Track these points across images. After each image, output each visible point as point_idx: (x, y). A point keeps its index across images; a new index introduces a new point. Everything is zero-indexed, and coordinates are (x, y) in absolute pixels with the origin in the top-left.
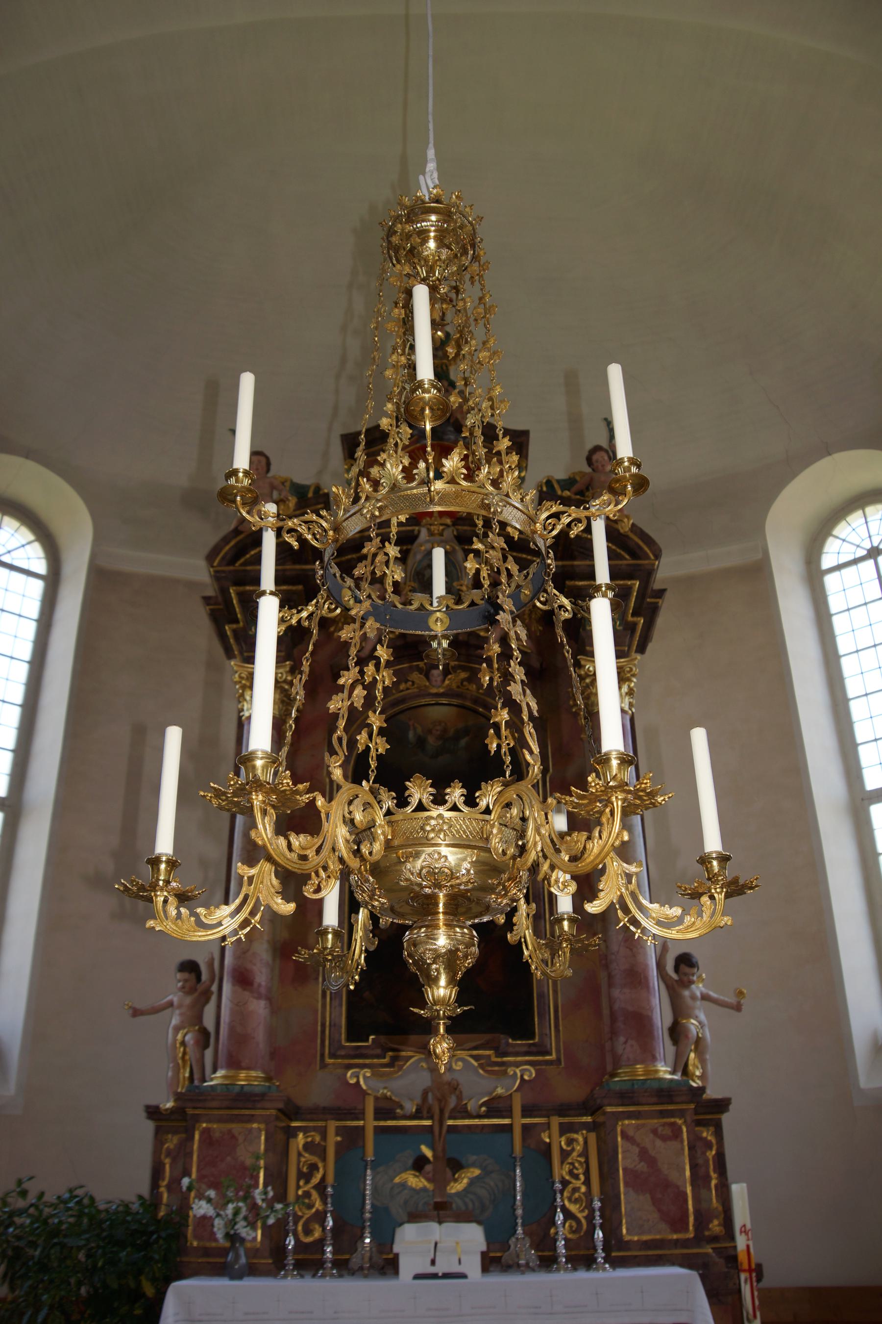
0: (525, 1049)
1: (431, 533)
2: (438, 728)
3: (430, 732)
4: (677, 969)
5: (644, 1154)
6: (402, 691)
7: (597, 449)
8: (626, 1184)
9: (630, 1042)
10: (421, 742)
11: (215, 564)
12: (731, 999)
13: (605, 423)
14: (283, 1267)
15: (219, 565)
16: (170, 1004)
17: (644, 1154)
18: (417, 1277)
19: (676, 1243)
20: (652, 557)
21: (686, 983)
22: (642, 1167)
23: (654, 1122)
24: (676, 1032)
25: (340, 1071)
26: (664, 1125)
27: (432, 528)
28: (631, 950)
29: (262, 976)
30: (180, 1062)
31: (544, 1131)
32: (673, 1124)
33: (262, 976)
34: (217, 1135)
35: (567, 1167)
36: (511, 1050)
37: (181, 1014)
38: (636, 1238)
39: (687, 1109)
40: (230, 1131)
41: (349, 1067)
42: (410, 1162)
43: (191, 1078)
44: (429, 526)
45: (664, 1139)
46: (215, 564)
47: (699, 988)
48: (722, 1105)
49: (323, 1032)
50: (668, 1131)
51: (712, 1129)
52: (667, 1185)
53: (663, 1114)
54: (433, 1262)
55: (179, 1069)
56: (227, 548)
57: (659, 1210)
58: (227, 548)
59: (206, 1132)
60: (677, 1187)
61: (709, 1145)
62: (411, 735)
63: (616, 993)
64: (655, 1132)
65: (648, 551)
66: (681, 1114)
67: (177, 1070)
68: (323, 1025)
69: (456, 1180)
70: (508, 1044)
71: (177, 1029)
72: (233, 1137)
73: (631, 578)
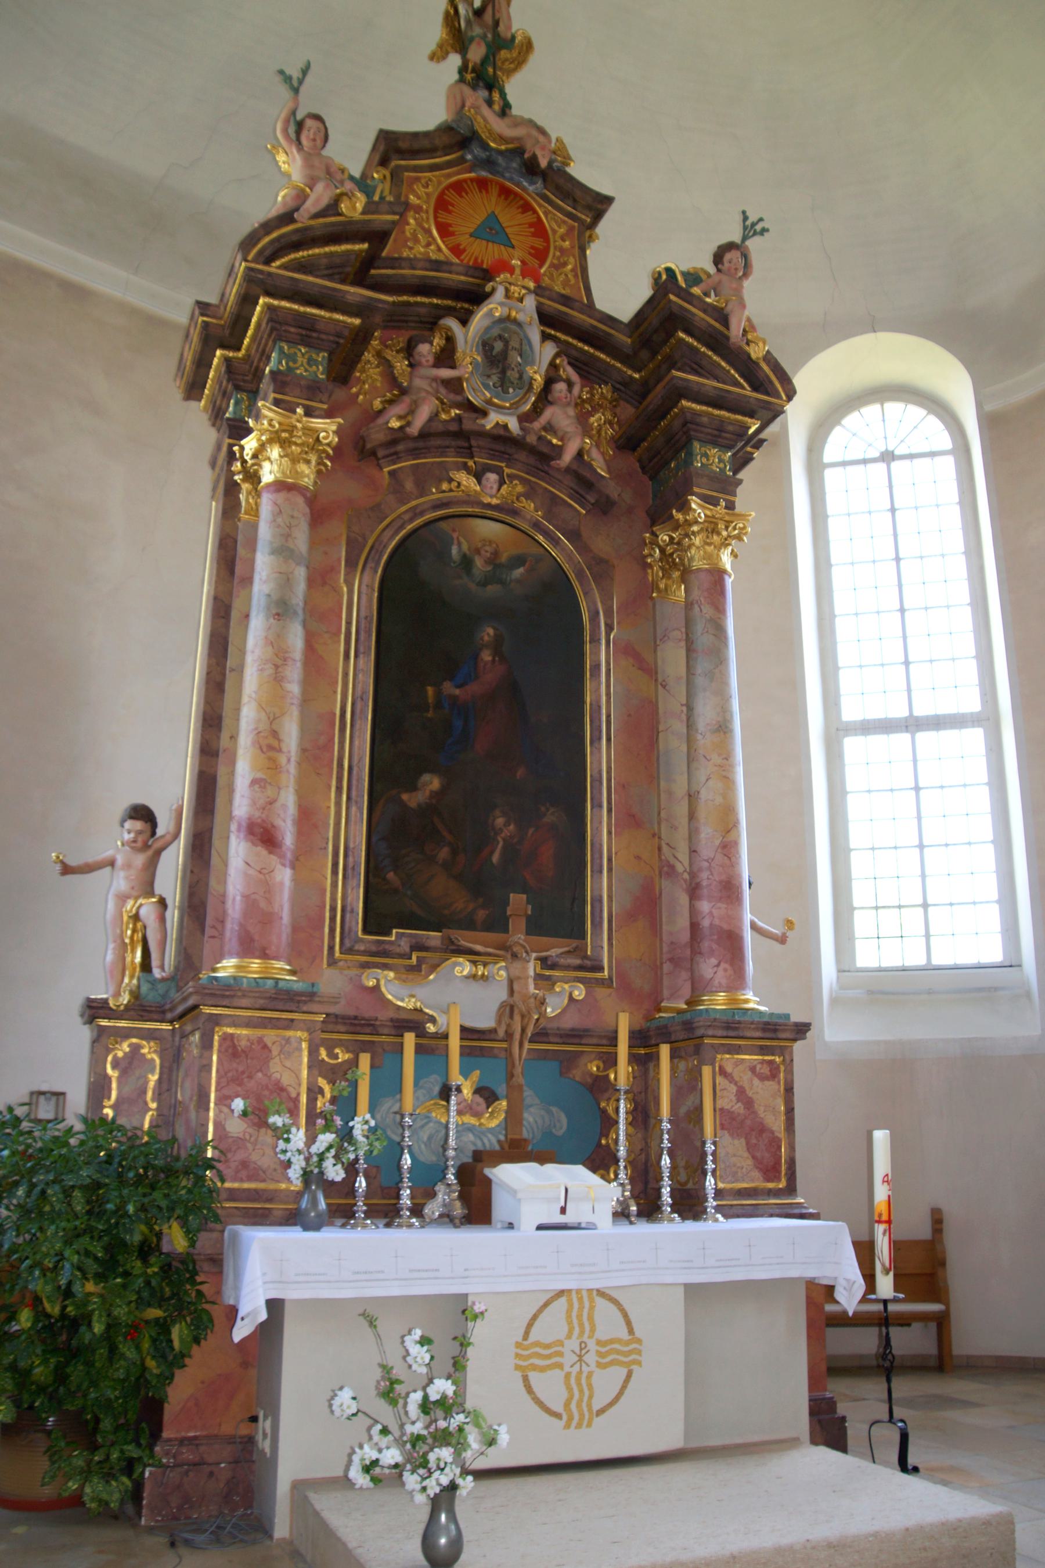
1: (508, 295)
2: (487, 548)
3: (478, 551)
5: (741, 1093)
6: (444, 492)
7: (730, 246)
9: (723, 965)
10: (467, 562)
11: (250, 258)
13: (742, 217)
14: (352, 1215)
17: (741, 1093)
18: (540, 1228)
20: (784, 397)
22: (739, 1108)
25: (354, 972)
26: (763, 1062)
27: (512, 288)
28: (730, 858)
30: (127, 941)
31: (591, 1062)
32: (771, 1062)
33: (288, 838)
34: (244, 1043)
37: (127, 878)
38: (729, 1186)
40: (260, 1040)
41: (365, 966)
42: (437, 1089)
44: (508, 285)
45: (762, 1078)
46: (250, 258)
49: (333, 919)
50: (766, 1070)
52: (762, 1129)
54: (563, 1211)
55: (125, 951)
56: (267, 240)
57: (754, 1157)
58: (267, 240)
59: (227, 1038)
60: (772, 1132)
62: (454, 550)
64: (753, 1069)
65: (780, 390)
68: (333, 909)
71: (123, 898)
72: (265, 1047)
73: (752, 415)
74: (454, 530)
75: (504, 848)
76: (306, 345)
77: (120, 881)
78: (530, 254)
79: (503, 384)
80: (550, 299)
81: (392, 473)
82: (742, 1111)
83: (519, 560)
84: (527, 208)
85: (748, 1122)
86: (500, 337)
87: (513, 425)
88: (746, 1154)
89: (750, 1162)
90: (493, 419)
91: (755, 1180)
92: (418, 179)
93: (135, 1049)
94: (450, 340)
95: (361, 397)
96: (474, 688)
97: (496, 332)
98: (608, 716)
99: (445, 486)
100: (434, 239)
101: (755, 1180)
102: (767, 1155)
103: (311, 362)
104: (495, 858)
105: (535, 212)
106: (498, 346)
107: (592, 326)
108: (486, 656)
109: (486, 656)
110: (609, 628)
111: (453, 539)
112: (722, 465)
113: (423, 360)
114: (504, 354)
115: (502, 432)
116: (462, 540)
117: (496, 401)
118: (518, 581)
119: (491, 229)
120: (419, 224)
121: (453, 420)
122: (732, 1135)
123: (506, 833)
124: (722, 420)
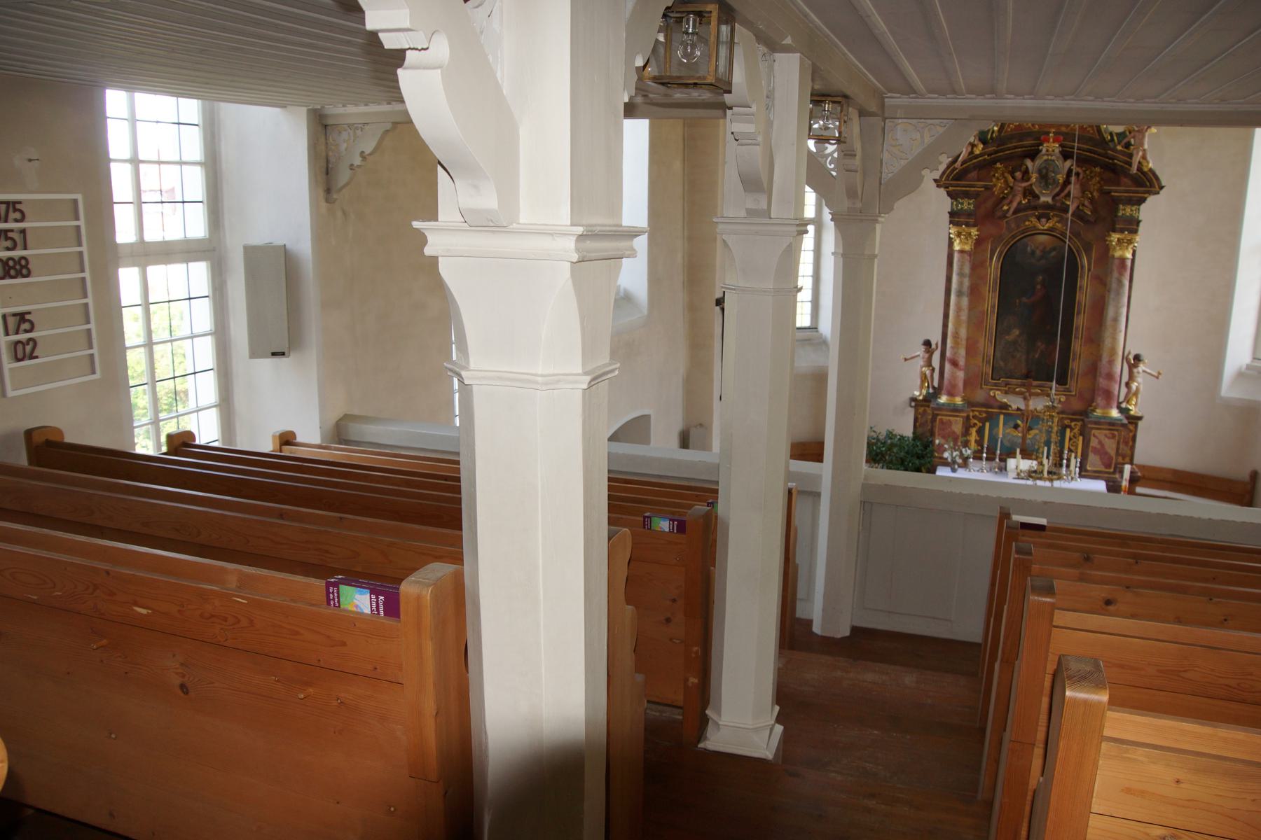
1: (1047, 151)
4: (1134, 360)
5: (1100, 443)
10: (1033, 253)
12: (1156, 374)
15: (945, 180)
16: (919, 356)
17: (1100, 443)
21: (1136, 366)
22: (1098, 447)
23: (1107, 432)
24: (1127, 385)
29: (962, 362)
33: (962, 362)
34: (944, 421)
35: (1072, 434)
41: (992, 389)
42: (1012, 425)
43: (928, 387)
45: (1109, 438)
47: (1141, 367)
48: (1140, 418)
50: (1111, 436)
51: (1134, 425)
52: (1106, 453)
61: (1131, 431)
62: (1029, 249)
63: (1101, 380)
64: (1106, 436)
67: (923, 382)
69: (1029, 434)
77: (922, 363)
81: (1007, 222)
83: (1054, 249)
86: (1045, 167)
89: (1100, 463)
90: (1043, 199)
91: (1102, 469)
93: (925, 410)
94: (1027, 168)
95: (996, 193)
97: (1043, 165)
99: (1027, 223)
101: (1102, 469)
103: (969, 204)
106: (1044, 171)
108: (1039, 287)
109: (1039, 287)
110: (1089, 270)
113: (1017, 179)
114: (1047, 174)
117: (1044, 192)
121: (1026, 203)
124: (1131, 197)
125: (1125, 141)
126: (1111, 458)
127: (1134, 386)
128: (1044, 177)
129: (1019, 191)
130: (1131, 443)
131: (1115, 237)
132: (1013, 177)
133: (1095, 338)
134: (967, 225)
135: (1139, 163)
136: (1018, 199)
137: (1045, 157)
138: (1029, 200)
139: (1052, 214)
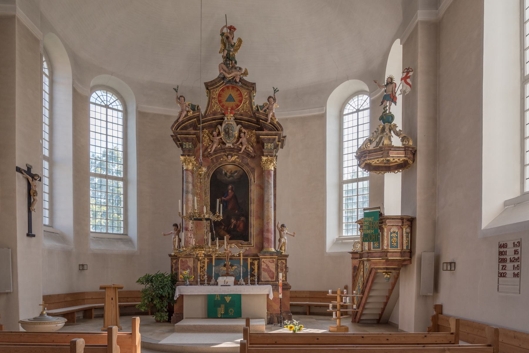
0: (247, 243)
5: (267, 265)
8: (263, 271)
10: (226, 174)
17: (267, 265)
18: (221, 286)
19: (272, 281)
22: (266, 268)
32: (273, 260)
36: (244, 244)
39: (276, 257)
45: (271, 263)
50: (272, 261)
52: (271, 271)
53: (271, 258)
62: (223, 172)
64: (269, 261)
66: (275, 258)
70: (243, 242)
73: (276, 135)
74: (223, 168)
75: (234, 225)
76: (188, 142)
78: (239, 102)
79: (229, 137)
80: (238, 116)
81: (211, 159)
82: (267, 268)
83: (236, 172)
84: (238, 90)
85: (268, 270)
87: (232, 146)
88: (267, 275)
89: (268, 276)
90: (227, 145)
92: (214, 91)
94: (219, 130)
95: (205, 145)
96: (228, 197)
97: (226, 127)
98: (254, 199)
100: (218, 104)
102: (272, 275)
103: (189, 145)
104: (232, 227)
105: (240, 91)
107: (248, 119)
108: (230, 191)
110: (254, 181)
111: (223, 170)
112: (271, 147)
115: (230, 147)
116: (225, 170)
117: (228, 141)
118: (236, 176)
119: (230, 98)
120: (215, 102)
122: (265, 272)
123: (234, 222)
125: (264, 109)
126: (273, 273)
127: (283, 240)
128: (227, 133)
129: (216, 142)
130: (284, 270)
131: (264, 158)
132: (213, 136)
133: (262, 216)
134: (189, 156)
135: (271, 118)
136: (215, 146)
137: (227, 122)
138: (221, 146)
139: (233, 154)
